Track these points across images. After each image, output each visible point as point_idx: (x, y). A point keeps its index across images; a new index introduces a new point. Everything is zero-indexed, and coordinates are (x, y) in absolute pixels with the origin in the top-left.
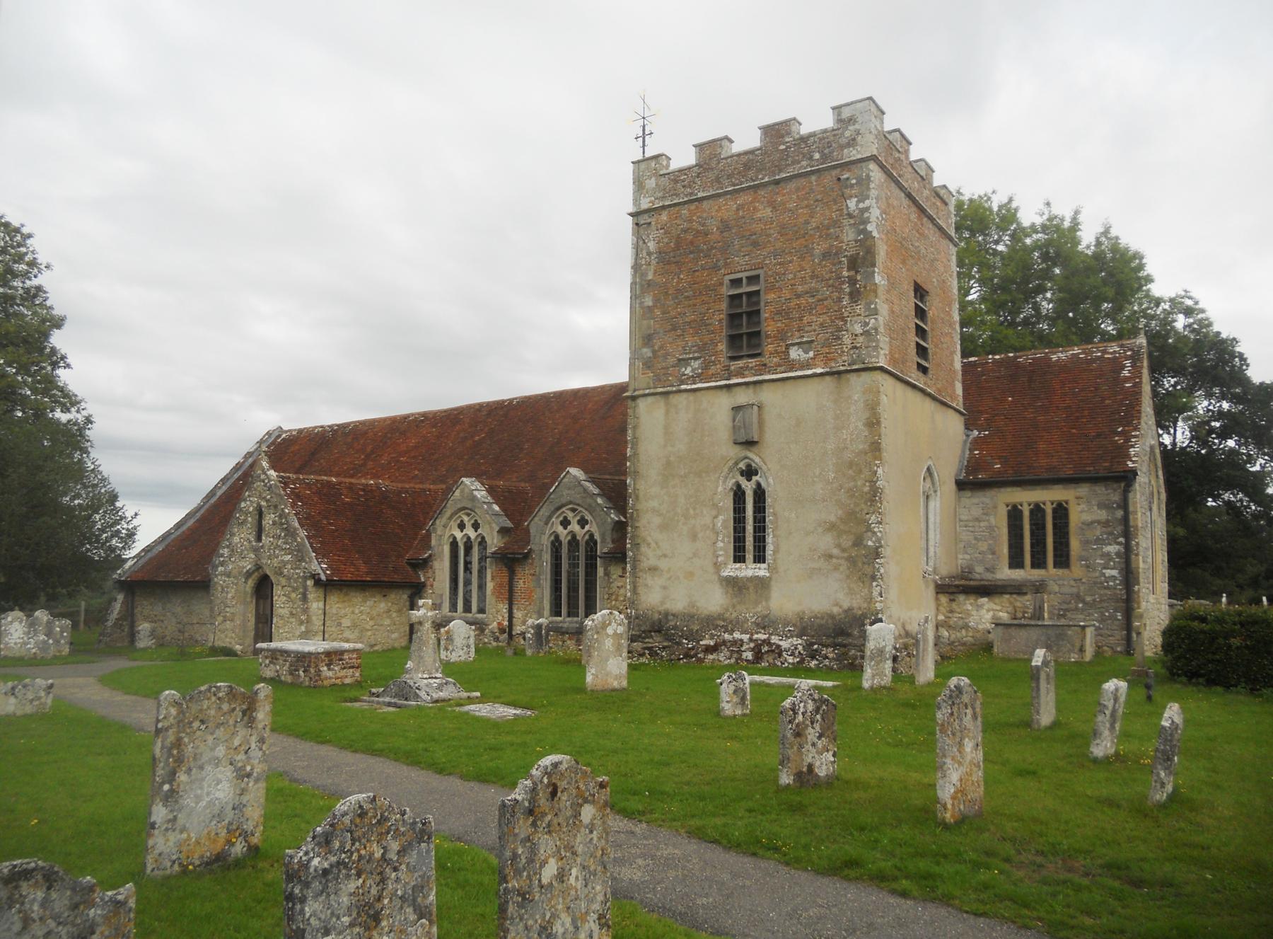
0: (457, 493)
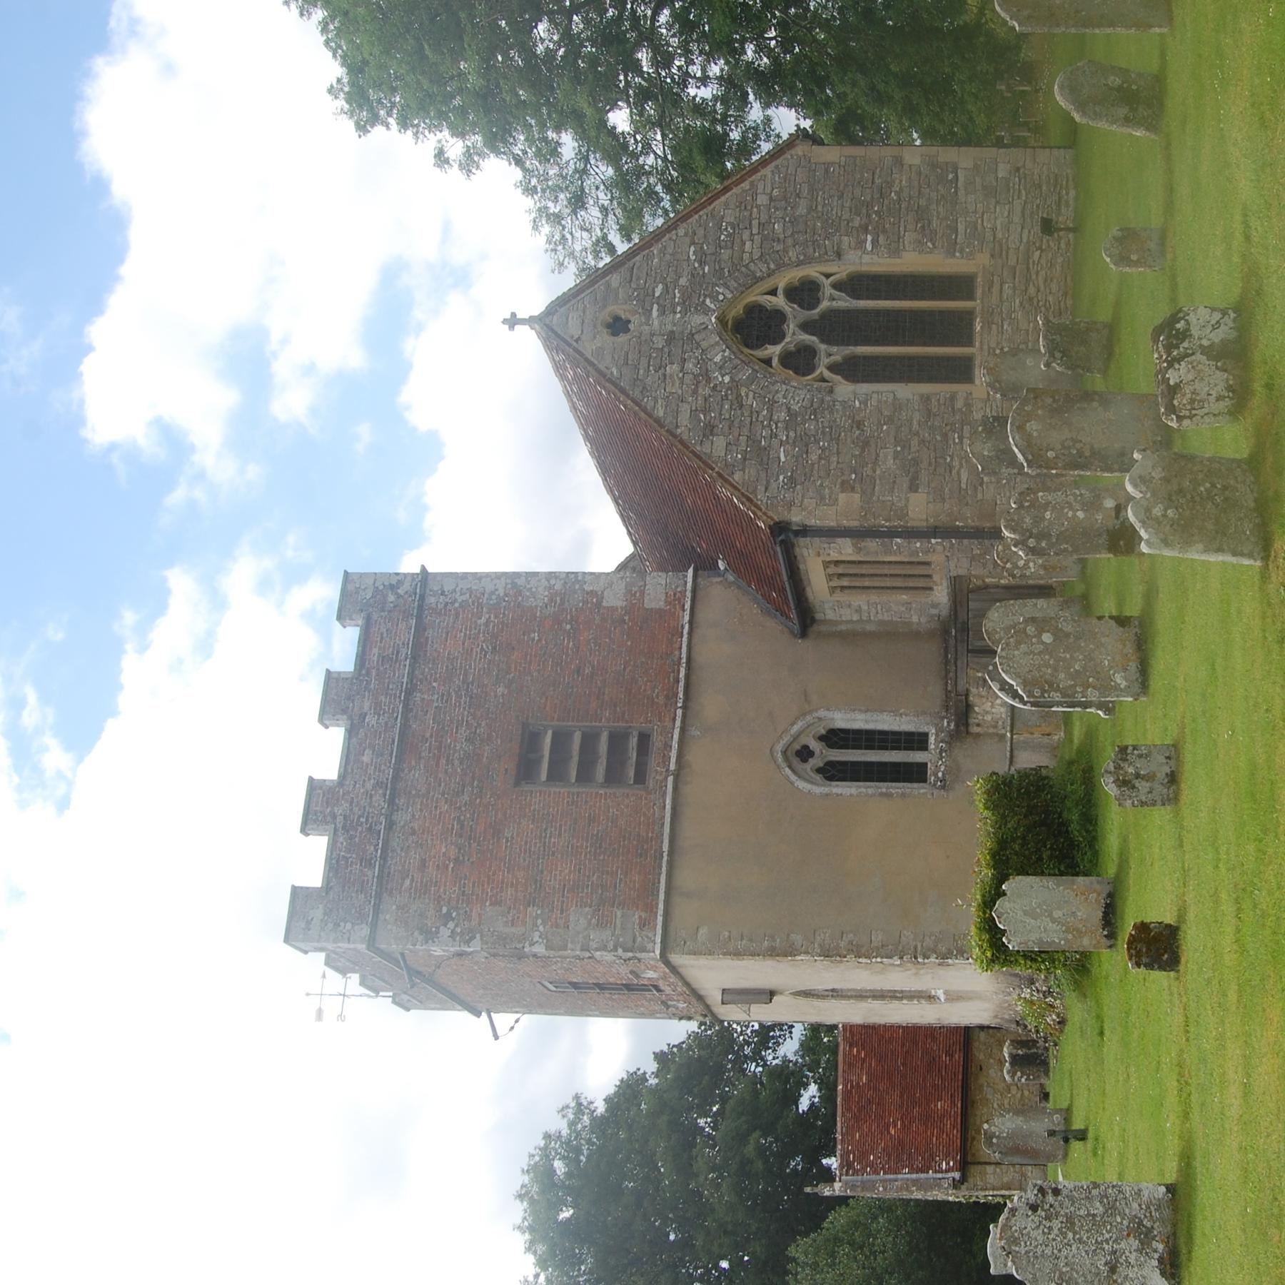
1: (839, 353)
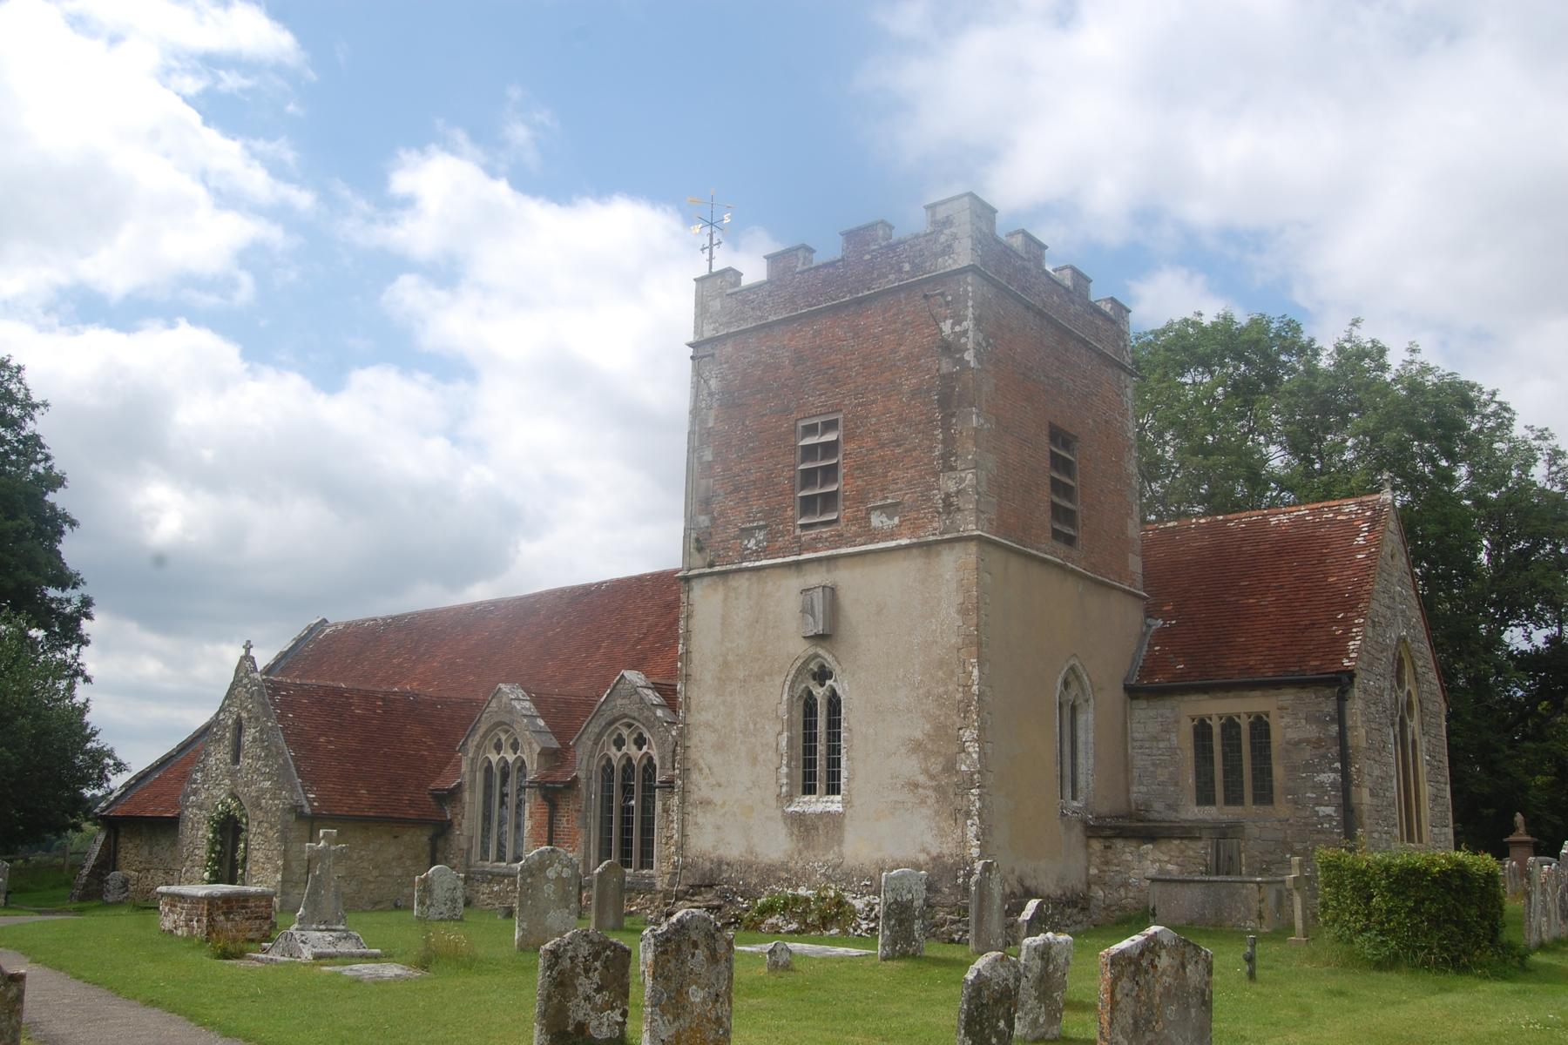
0: (494, 704)
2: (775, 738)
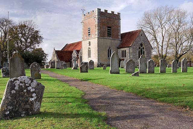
1: (140, 51)
2: (87, 53)
